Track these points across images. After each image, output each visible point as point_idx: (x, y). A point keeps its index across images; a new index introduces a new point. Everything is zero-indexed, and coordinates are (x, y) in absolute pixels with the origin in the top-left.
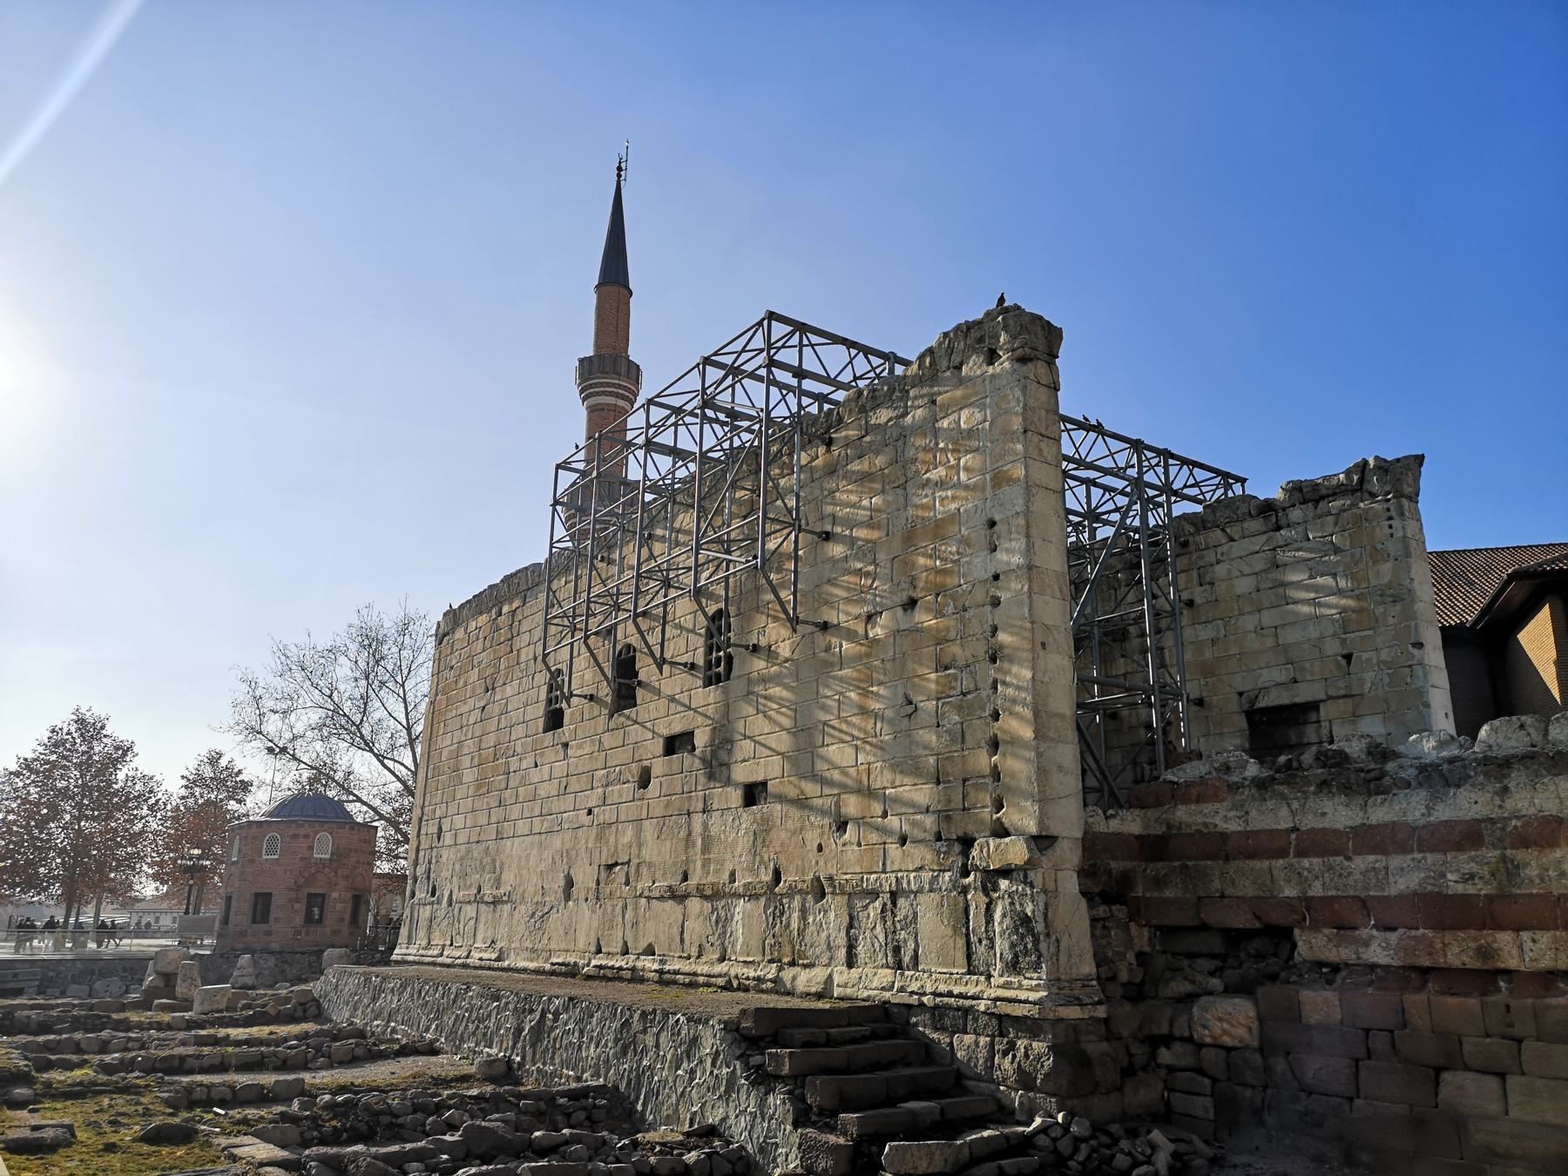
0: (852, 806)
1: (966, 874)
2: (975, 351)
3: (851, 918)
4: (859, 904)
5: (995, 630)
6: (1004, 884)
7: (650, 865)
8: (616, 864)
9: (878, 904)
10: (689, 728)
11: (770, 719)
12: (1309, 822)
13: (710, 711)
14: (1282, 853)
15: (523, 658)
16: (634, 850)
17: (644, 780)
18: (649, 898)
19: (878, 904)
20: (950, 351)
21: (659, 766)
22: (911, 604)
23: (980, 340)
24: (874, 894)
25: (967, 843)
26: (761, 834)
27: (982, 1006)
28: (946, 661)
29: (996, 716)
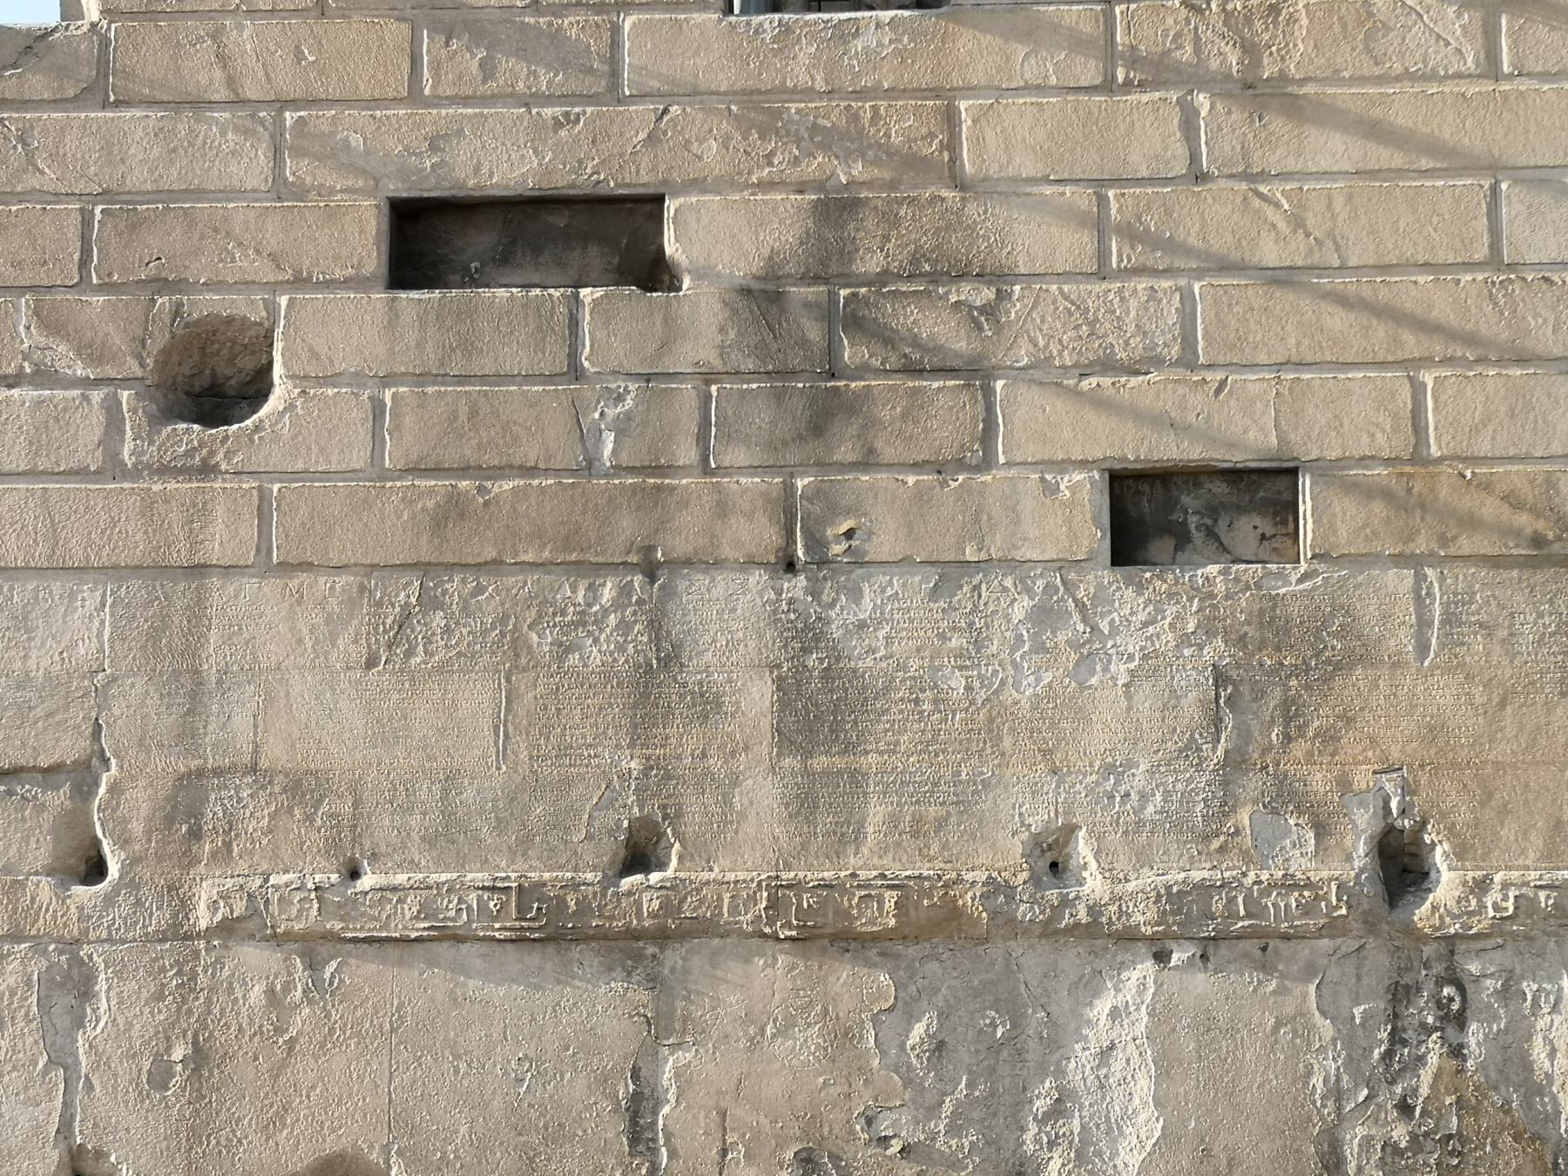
7: (302, 789)
10: (640, 177)
16: (136, 705)
17: (214, 385)
18: (313, 947)
21: (339, 339)
26: (1269, 692)
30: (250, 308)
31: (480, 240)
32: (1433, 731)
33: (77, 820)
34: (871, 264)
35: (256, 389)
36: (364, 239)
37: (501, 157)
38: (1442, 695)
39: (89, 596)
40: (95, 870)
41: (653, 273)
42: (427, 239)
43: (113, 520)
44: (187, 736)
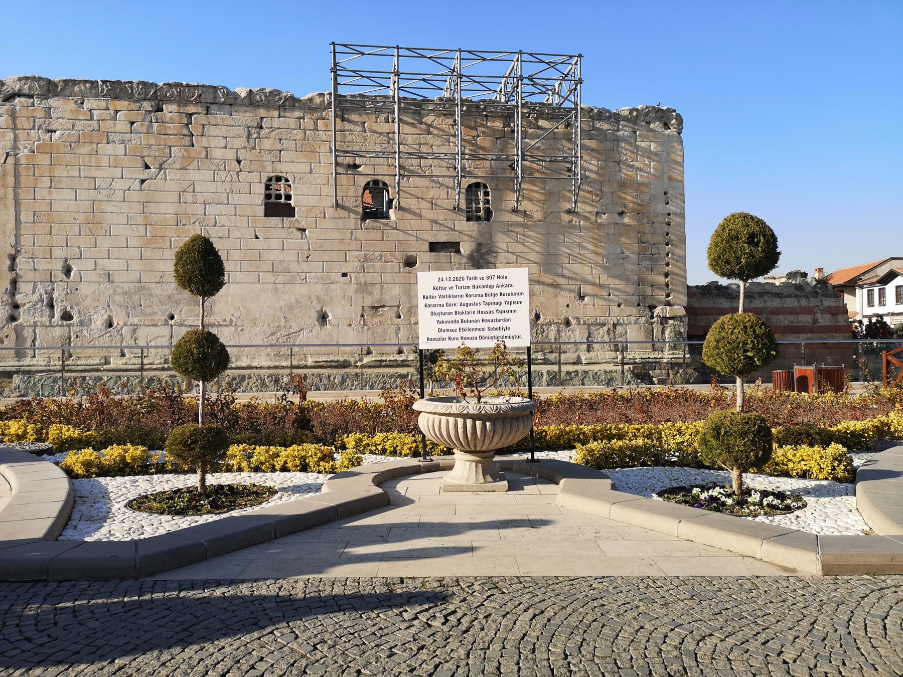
0: (586, 289)
1: (652, 317)
2: (658, 120)
3: (590, 334)
4: (593, 328)
5: (667, 234)
6: (671, 322)
8: (384, 306)
9: (606, 328)
10: (458, 240)
11: (529, 248)
12: (717, 306)
13: (475, 234)
14: (712, 314)
15: (217, 154)
16: (404, 299)
19: (606, 328)
20: (647, 114)
22: (621, 214)
23: (662, 117)
24: (604, 325)
25: (652, 308)
27: (665, 361)
28: (644, 240)
29: (668, 265)
30: (414, 254)
31: (439, 247)
32: (541, 303)
33: (398, 312)
34: (483, 251)
35: (414, 263)
36: (427, 247)
37: (442, 238)
38: (542, 299)
39: (398, 286)
40: (400, 317)
41: (458, 251)
42: (434, 247)
43: (400, 278)
44: (410, 303)
